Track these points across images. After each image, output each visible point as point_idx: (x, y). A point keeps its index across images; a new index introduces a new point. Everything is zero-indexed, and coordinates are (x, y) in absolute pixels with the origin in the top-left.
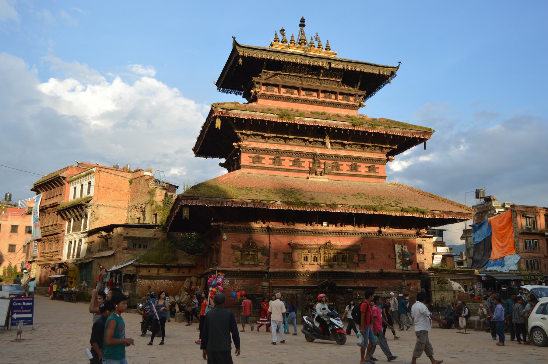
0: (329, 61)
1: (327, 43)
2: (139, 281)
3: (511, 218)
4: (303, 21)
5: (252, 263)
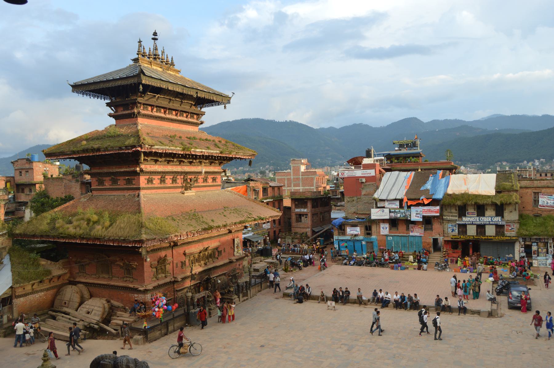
0: (196, 91)
1: (172, 59)
2: (16, 302)
3: (246, 191)
4: (155, 34)
5: (164, 275)
